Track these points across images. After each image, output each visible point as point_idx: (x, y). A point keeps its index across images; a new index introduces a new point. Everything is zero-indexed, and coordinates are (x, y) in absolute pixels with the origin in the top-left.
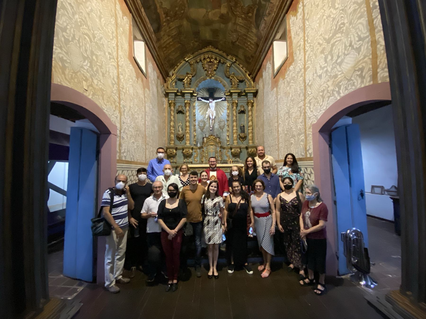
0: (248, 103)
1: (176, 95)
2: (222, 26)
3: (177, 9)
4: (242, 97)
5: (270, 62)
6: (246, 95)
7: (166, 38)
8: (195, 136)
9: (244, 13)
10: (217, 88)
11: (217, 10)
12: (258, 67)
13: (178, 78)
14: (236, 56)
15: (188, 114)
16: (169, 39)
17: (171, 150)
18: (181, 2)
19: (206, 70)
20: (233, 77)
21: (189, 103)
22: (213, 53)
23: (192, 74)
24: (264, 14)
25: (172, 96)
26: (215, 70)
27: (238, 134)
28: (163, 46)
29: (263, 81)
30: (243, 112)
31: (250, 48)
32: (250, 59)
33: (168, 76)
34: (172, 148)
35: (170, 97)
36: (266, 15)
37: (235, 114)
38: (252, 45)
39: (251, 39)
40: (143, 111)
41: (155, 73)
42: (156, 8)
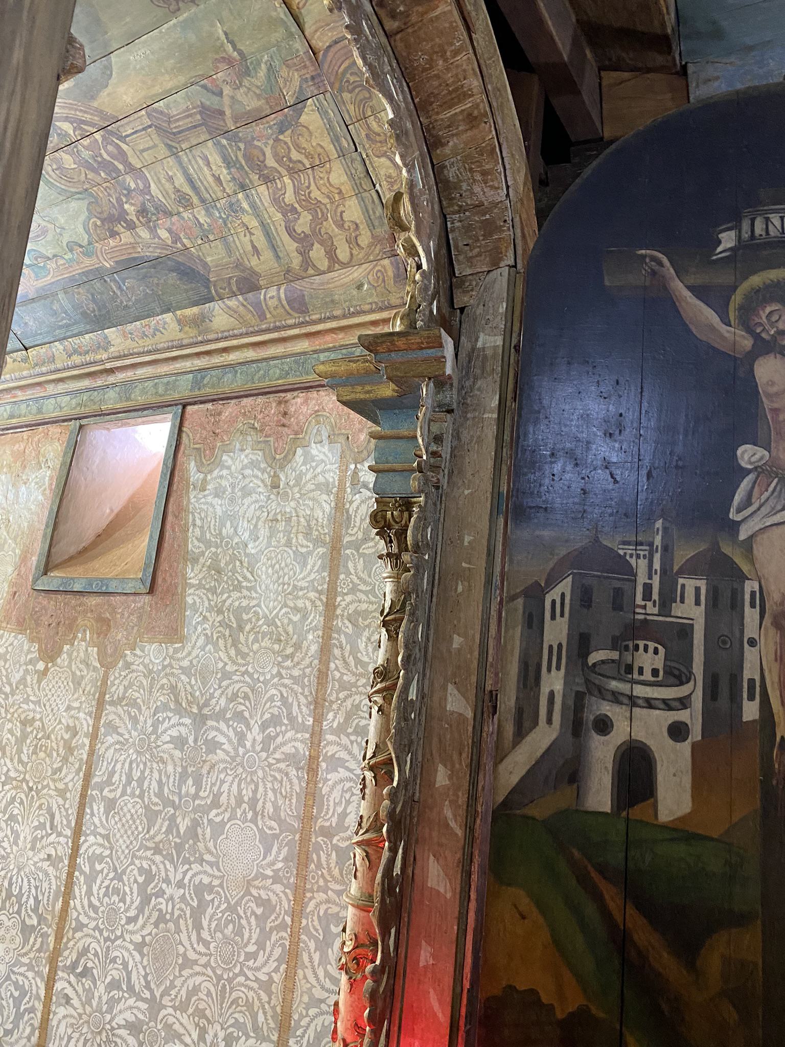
40: (62, 793)
42: (98, 274)
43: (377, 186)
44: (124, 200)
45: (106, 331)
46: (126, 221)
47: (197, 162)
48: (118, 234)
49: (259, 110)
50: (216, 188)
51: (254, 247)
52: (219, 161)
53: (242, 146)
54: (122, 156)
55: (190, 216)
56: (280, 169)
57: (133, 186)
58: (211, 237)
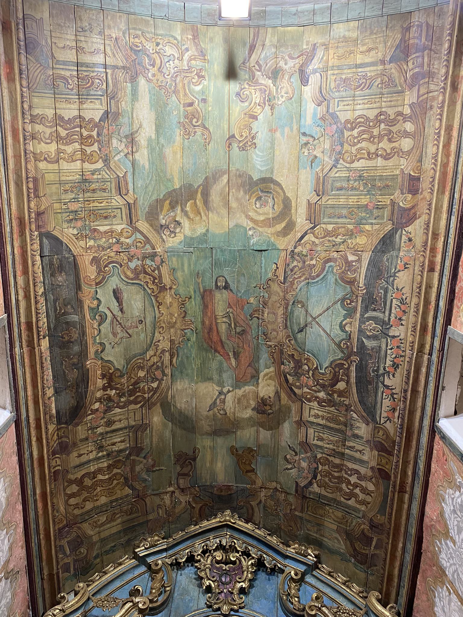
2: (265, 435)
3: (141, 374)
7: (89, 452)
9: (323, 386)
11: (247, 388)
12: (408, 558)
14: (318, 544)
18: (155, 359)
19: (209, 589)
20: (319, 609)
22: (236, 535)
23: (151, 601)
24: (381, 371)
26: (242, 591)
28: (72, 477)
31: (362, 496)
32: (369, 540)
36: (389, 372)
38: (363, 483)
42: (83, 354)
43: (96, 516)
44: (117, 392)
45: (47, 337)
46: (107, 387)
47: (123, 436)
48: (103, 379)
49: (134, 471)
50: (111, 442)
51: (82, 455)
52: (121, 448)
53: (124, 460)
54: (135, 402)
55: (102, 424)
56: (111, 474)
57: (122, 400)
58: (90, 432)
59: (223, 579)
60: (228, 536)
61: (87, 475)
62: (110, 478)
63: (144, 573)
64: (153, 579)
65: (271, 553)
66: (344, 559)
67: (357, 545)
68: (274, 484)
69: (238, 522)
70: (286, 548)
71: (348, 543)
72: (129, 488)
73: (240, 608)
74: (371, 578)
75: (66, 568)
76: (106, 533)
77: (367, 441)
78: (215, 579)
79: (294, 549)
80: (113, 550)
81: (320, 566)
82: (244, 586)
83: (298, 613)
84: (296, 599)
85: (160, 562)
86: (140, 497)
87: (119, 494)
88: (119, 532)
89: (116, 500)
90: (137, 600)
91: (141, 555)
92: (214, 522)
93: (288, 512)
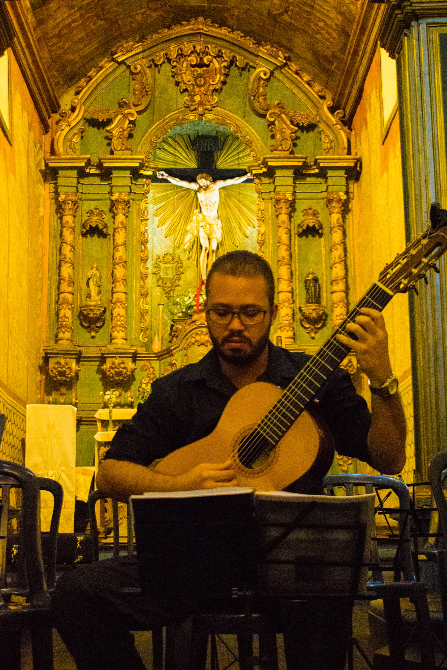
0: (329, 201)
1: (82, 173)
4: (309, 180)
5: (376, 93)
6: (323, 173)
8: (143, 314)
10: (227, 137)
13: (88, 116)
15: (120, 238)
16: (70, 15)
17: (62, 361)
19: (186, 90)
21: (127, 203)
22: (208, 39)
25: (67, 180)
26: (215, 90)
27: (298, 305)
28: (50, 35)
29: (368, 137)
30: (312, 231)
31: (326, 36)
32: (331, 63)
33: (56, 112)
34: (66, 354)
35: (60, 181)
37: (285, 238)
38: (329, 30)
39: (323, 14)
41: (25, 114)
59: (198, 83)
60: (202, 42)
61: (64, 27)
62: (83, 22)
63: (124, 72)
64: (134, 79)
65: (243, 52)
66: (309, 63)
67: (321, 61)
68: (247, 7)
69: (211, 28)
70: (258, 49)
71: (314, 57)
72: (101, 20)
73: (213, 107)
74: (330, 82)
75: (58, 84)
76: (87, 52)
77: (334, 7)
78: (190, 83)
79: (266, 49)
80: (92, 59)
81: (289, 63)
82: (217, 88)
83: (262, 112)
84: (263, 98)
85: (139, 67)
86: (114, 22)
87: (93, 27)
88: (97, 48)
89: (91, 31)
90: (126, 111)
91: (120, 60)
92: (186, 29)
93: (261, 24)
